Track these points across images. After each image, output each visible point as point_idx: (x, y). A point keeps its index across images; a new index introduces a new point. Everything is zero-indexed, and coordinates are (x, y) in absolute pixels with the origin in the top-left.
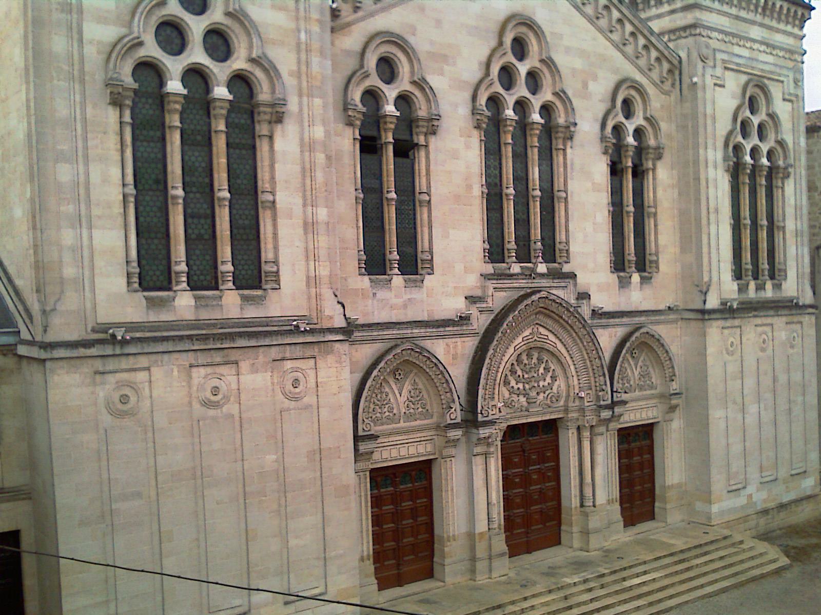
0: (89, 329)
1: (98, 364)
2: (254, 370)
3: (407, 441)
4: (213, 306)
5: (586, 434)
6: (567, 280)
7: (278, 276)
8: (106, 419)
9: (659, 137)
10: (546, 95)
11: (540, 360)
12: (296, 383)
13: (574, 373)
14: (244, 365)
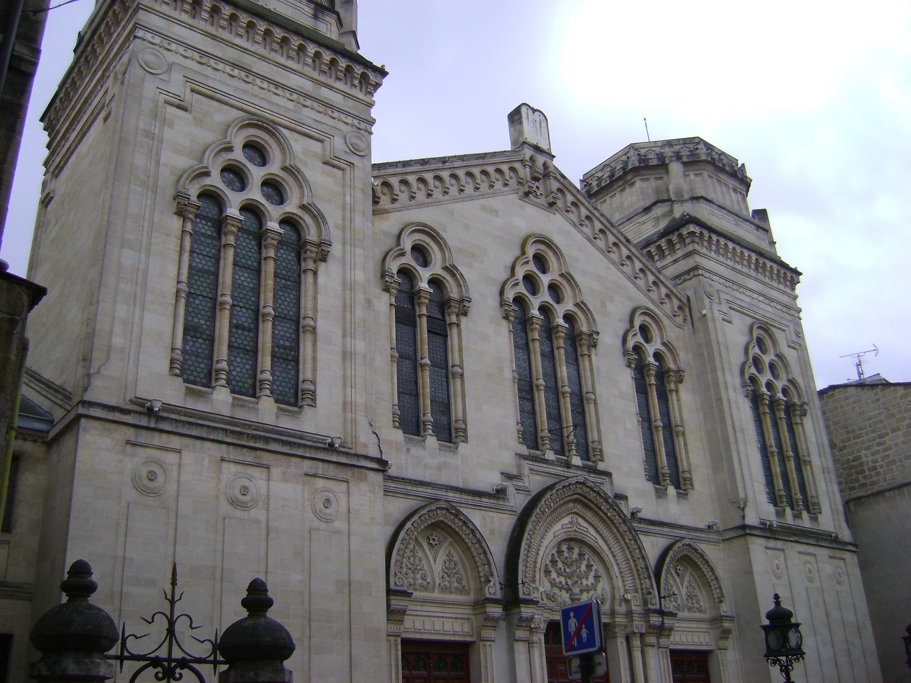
0: (128, 399)
1: (130, 433)
2: (285, 479)
3: (441, 615)
4: (249, 407)
5: (636, 643)
6: (603, 477)
7: (315, 396)
8: (130, 494)
9: (678, 362)
10: (568, 305)
11: (581, 555)
12: (328, 502)
13: (618, 574)
14: (276, 472)
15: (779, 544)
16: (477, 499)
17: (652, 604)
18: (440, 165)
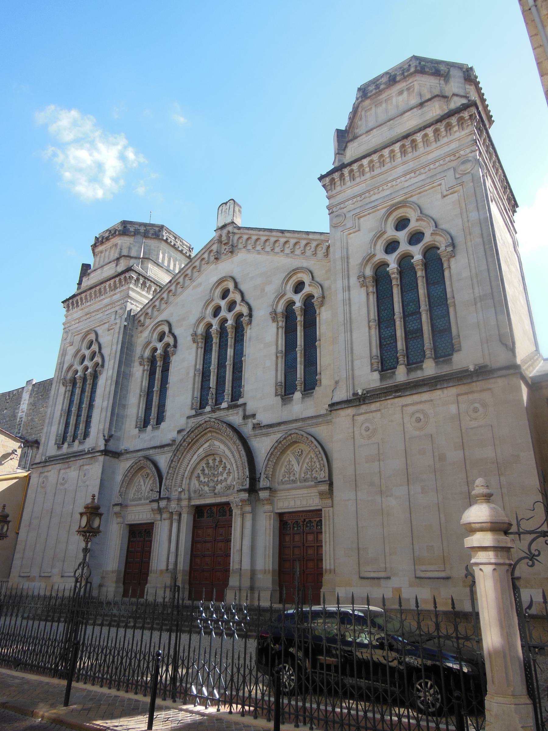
14: (72, 468)
15: (374, 407)
16: (162, 449)
17: (242, 486)
18: (169, 284)
